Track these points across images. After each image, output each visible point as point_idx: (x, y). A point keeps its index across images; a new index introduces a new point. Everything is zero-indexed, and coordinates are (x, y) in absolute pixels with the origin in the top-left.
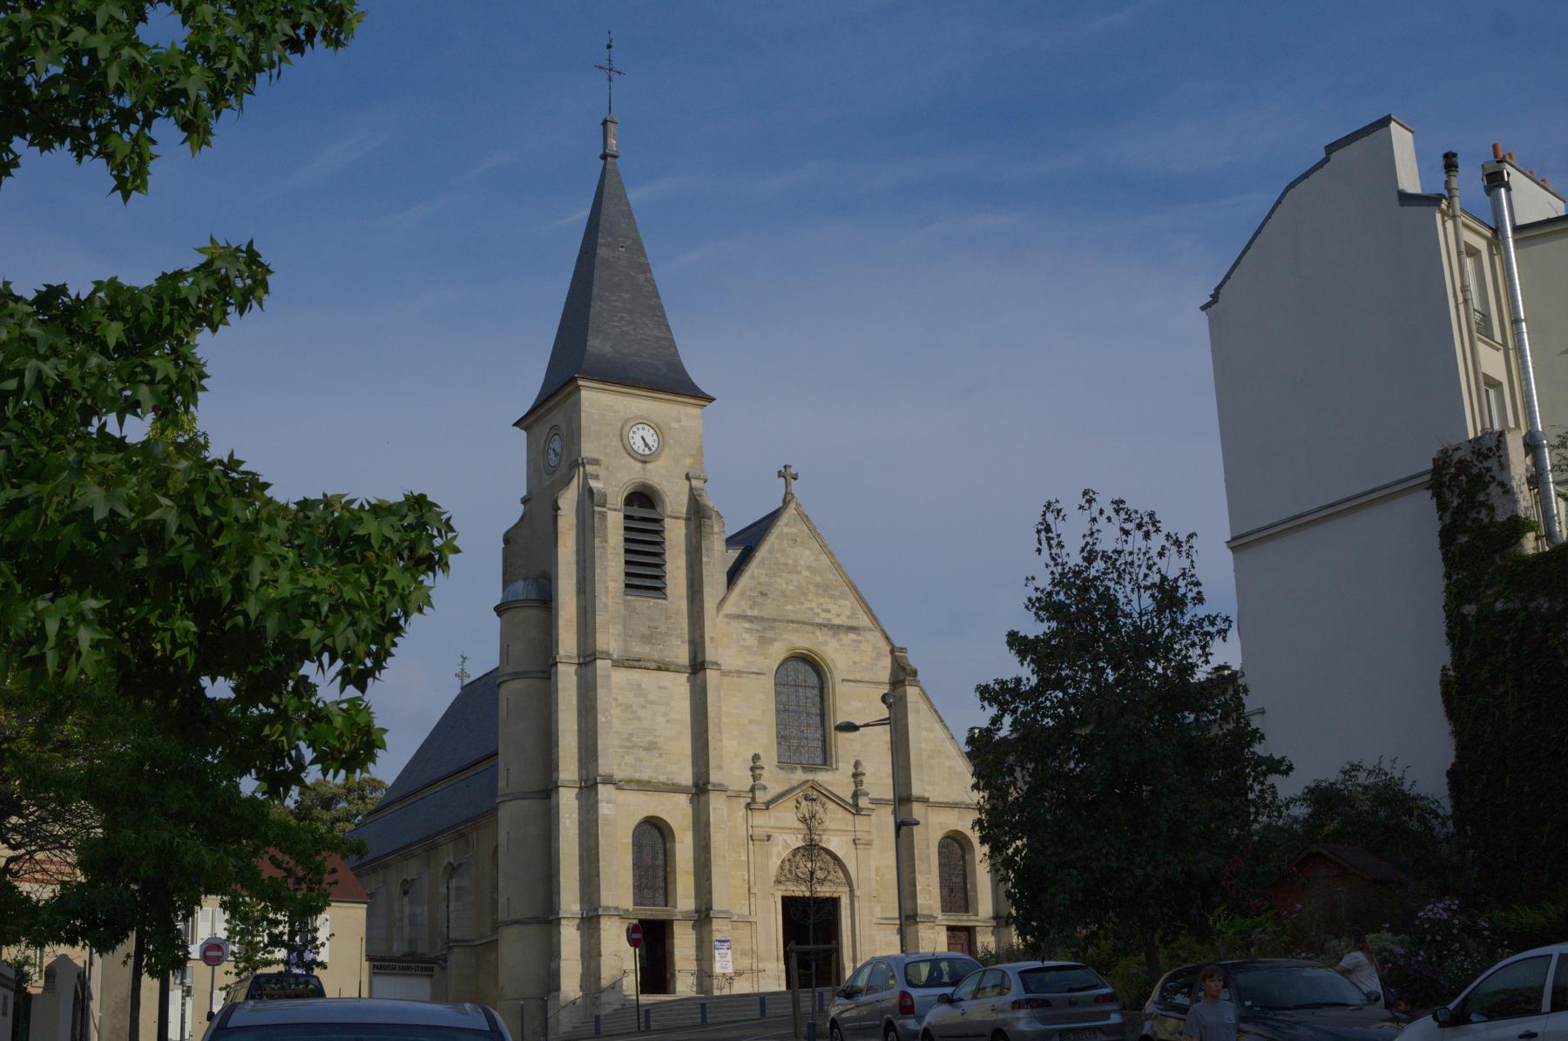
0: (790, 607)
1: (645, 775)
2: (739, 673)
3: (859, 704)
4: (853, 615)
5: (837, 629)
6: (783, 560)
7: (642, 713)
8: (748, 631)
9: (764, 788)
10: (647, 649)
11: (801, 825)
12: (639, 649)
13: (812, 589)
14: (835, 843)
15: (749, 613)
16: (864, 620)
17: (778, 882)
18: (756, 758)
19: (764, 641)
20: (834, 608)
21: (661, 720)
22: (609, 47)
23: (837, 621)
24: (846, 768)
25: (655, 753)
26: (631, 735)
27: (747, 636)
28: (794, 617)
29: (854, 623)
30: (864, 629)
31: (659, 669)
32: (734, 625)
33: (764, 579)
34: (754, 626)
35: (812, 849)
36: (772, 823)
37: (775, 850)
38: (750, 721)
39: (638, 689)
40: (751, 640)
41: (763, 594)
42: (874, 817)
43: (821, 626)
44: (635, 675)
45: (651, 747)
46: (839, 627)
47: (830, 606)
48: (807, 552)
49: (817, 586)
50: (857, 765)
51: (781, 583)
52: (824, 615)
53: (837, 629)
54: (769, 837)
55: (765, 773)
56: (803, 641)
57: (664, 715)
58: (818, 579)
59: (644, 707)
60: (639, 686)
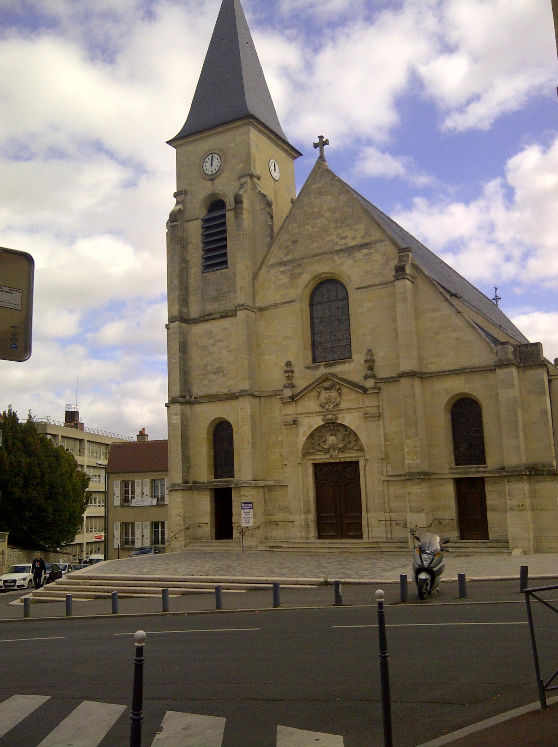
0: (315, 245)
1: (214, 390)
2: (276, 305)
3: (371, 304)
4: (367, 233)
5: (349, 250)
6: (310, 211)
7: (212, 349)
8: (283, 272)
9: (293, 386)
10: (216, 305)
11: (321, 410)
12: (212, 307)
13: (332, 225)
14: (349, 420)
15: (285, 259)
16: (376, 235)
17: (306, 454)
18: (288, 364)
19: (294, 277)
20: (350, 234)
21: (224, 351)
23: (353, 243)
24: (359, 357)
25: (221, 375)
26: (206, 366)
27: (281, 277)
28: (318, 252)
29: (367, 240)
30: (375, 242)
31: (222, 317)
32: (273, 271)
33: (296, 230)
34: (289, 267)
35: (332, 426)
36: (300, 410)
38: (286, 338)
40: (284, 279)
41: (294, 242)
43: (338, 252)
44: (208, 325)
45: (219, 371)
46: (353, 248)
48: (329, 198)
49: (336, 221)
51: (309, 229)
52: (343, 242)
53: (349, 250)
54: (295, 422)
55: (296, 375)
56: (323, 268)
57: (226, 348)
58: (338, 215)
59: (214, 345)
60: (211, 332)
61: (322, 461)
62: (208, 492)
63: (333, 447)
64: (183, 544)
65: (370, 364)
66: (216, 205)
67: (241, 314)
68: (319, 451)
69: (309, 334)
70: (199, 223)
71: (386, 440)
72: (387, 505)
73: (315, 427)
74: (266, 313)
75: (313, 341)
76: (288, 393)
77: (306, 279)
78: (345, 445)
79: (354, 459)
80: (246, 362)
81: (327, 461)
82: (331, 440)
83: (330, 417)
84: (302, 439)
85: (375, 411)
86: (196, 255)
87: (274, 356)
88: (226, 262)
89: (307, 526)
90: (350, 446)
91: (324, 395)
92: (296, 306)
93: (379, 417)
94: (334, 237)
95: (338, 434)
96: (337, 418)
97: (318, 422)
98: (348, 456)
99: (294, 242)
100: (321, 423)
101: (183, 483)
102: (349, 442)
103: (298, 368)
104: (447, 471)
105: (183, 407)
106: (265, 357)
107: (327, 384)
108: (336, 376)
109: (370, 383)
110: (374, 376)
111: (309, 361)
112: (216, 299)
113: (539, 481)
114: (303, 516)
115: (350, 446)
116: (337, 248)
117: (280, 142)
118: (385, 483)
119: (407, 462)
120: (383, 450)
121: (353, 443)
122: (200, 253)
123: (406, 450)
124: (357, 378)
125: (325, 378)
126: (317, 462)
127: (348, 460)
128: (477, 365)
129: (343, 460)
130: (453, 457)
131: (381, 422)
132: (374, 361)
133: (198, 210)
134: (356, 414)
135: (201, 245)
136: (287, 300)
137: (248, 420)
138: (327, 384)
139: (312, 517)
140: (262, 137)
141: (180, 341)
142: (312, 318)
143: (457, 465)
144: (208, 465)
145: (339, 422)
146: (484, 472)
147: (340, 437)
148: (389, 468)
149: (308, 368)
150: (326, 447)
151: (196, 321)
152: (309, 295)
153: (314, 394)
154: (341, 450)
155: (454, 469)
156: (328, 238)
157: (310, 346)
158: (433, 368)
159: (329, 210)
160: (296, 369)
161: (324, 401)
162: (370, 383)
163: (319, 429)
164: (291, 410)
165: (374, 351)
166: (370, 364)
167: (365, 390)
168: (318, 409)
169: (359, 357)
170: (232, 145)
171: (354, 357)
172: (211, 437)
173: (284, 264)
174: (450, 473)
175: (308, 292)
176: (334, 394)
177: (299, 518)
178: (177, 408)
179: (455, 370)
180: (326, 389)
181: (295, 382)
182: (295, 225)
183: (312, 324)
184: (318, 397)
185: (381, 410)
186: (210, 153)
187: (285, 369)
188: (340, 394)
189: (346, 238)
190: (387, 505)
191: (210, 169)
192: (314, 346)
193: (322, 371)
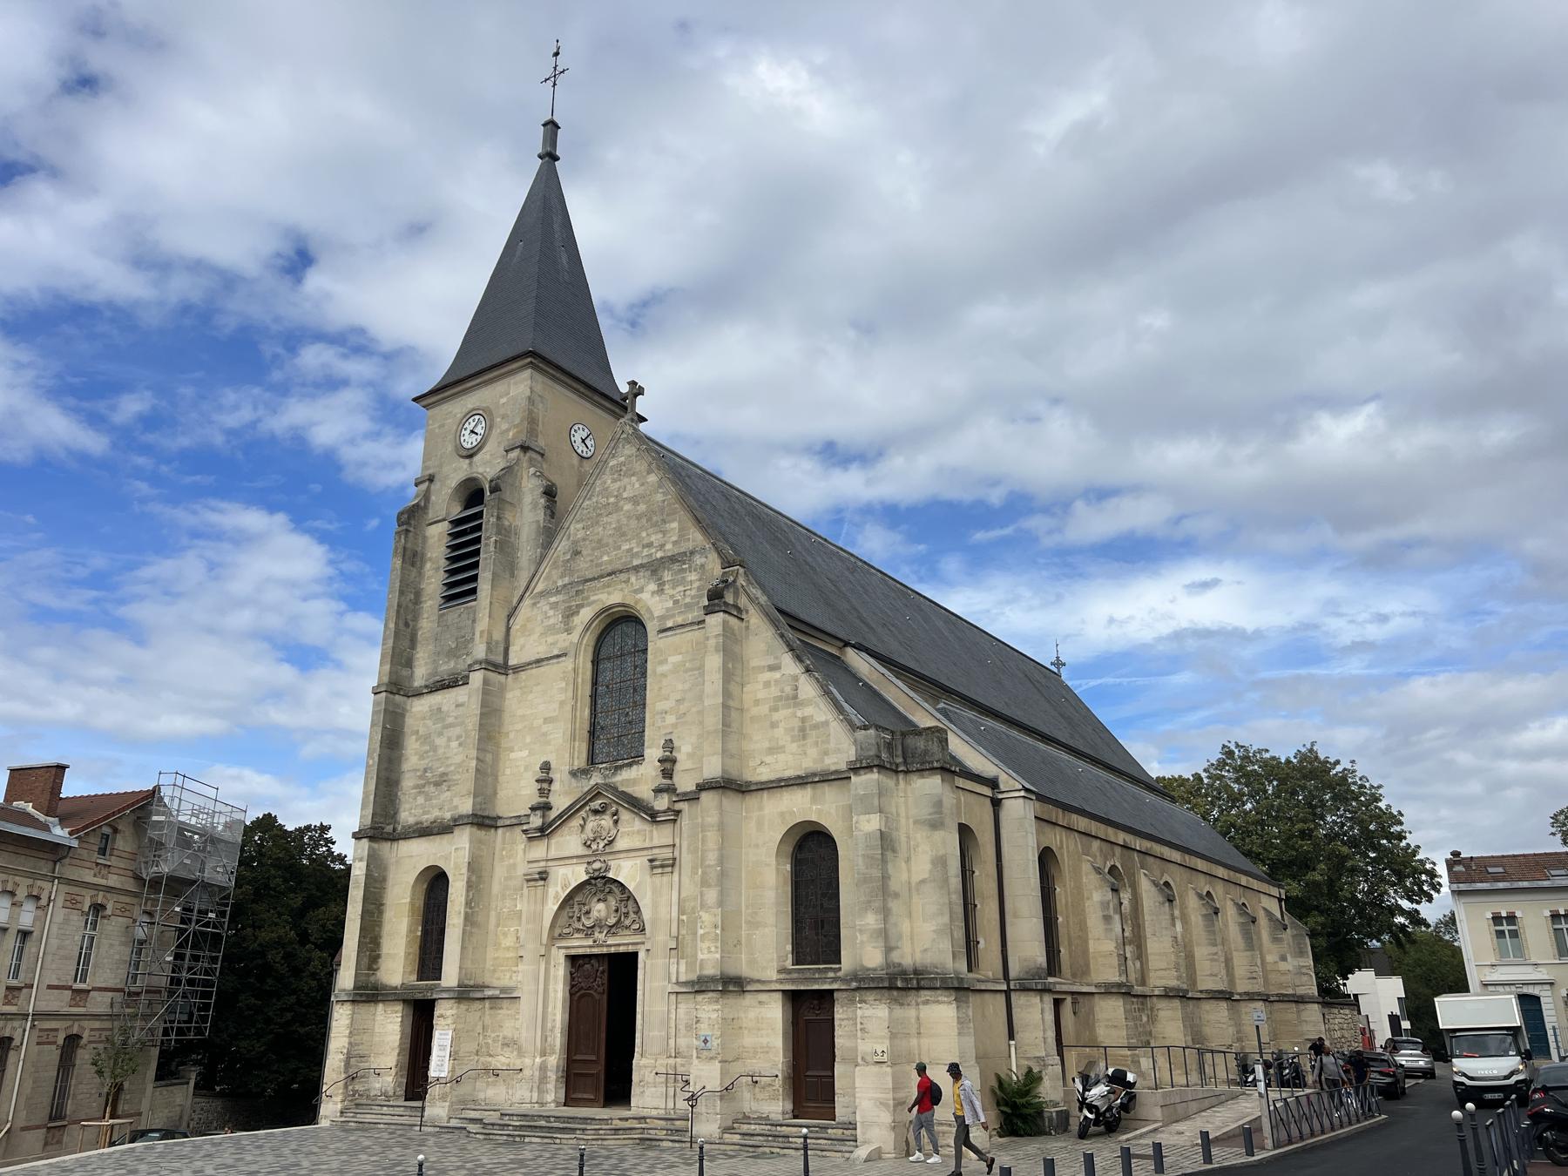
0: (605, 558)
2: (538, 661)
8: (554, 606)
12: (447, 667)
13: (633, 523)
14: (627, 871)
15: (560, 583)
17: (555, 937)
18: (546, 767)
19: (570, 614)
20: (655, 538)
21: (454, 744)
22: (556, 54)
24: (653, 753)
25: (444, 787)
26: (425, 771)
27: (551, 613)
28: (610, 569)
33: (580, 535)
35: (600, 884)
36: (553, 854)
37: (551, 891)
38: (546, 720)
39: (438, 711)
40: (556, 618)
42: (685, 821)
43: (636, 569)
47: (653, 538)
48: (634, 479)
49: (638, 518)
50: (669, 745)
52: (645, 552)
53: (654, 568)
54: (543, 876)
55: (555, 787)
56: (612, 596)
58: (642, 507)
59: (440, 734)
60: (439, 709)
61: (581, 951)
62: (399, 1007)
63: (599, 925)
64: (339, 1106)
65: (668, 765)
66: (473, 494)
67: (477, 678)
68: (578, 930)
69: (587, 712)
70: (444, 527)
71: (681, 911)
72: (672, 1042)
73: (574, 885)
74: (523, 675)
75: (593, 725)
76: (536, 821)
77: (586, 614)
78: (619, 921)
79: (631, 949)
80: (474, 763)
81: (588, 951)
82: (599, 909)
83: (597, 865)
84: (552, 907)
85: (667, 853)
86: (434, 580)
87: (525, 753)
88: (474, 591)
89: (543, 1079)
90: (627, 922)
91: (592, 824)
92: (567, 664)
93: (673, 865)
94: (633, 544)
95: (610, 898)
96: (607, 869)
97: (578, 874)
98: (619, 943)
99: (577, 553)
100: (585, 877)
101: (355, 988)
102: (626, 915)
103: (560, 775)
104: (775, 976)
105: (375, 846)
106: (513, 755)
107: (596, 804)
108: (613, 789)
109: (662, 803)
110: (670, 790)
111: (580, 761)
112: (453, 654)
113: (926, 1002)
114: (538, 1060)
115: (627, 922)
116: (636, 562)
117: (596, 398)
118: (673, 997)
119: (700, 956)
120: (674, 933)
121: (632, 915)
122: (442, 575)
123: (701, 932)
124: (644, 791)
125: (596, 793)
126: (573, 952)
127: (622, 949)
128: (833, 768)
129: (613, 950)
130: (789, 948)
131: (676, 876)
132: (674, 761)
133: (444, 504)
134: (638, 861)
135: (443, 563)
136: (556, 652)
137: (464, 870)
138: (596, 804)
139: (555, 1060)
140: (558, 387)
141: (384, 728)
142: (595, 683)
143: (797, 961)
144: (407, 954)
145: (610, 875)
146: (835, 980)
147: (613, 903)
148: (683, 968)
149: (573, 774)
150: (589, 923)
151: (418, 694)
152: (592, 643)
153: (576, 822)
154: (612, 929)
155: (789, 972)
156: (626, 547)
157: (586, 735)
158: (765, 774)
159: (629, 499)
160: (554, 775)
161: (591, 836)
162: (662, 803)
163: (580, 887)
164: (539, 850)
165: (676, 743)
166: (668, 765)
167: (653, 816)
168: (581, 851)
169: (653, 753)
170: (504, 400)
171: (647, 752)
172: (420, 903)
173: (558, 592)
174: (780, 981)
175: (590, 640)
176: (606, 821)
177: (531, 1063)
178: (365, 843)
179: (799, 777)
180: (596, 812)
181: (553, 799)
182: (580, 526)
183: (594, 697)
184: (583, 827)
185: (677, 854)
186: (470, 415)
187: (540, 775)
188: (616, 822)
189: (650, 545)
190: (672, 1042)
191: (469, 441)
192: (592, 733)
193: (596, 779)
